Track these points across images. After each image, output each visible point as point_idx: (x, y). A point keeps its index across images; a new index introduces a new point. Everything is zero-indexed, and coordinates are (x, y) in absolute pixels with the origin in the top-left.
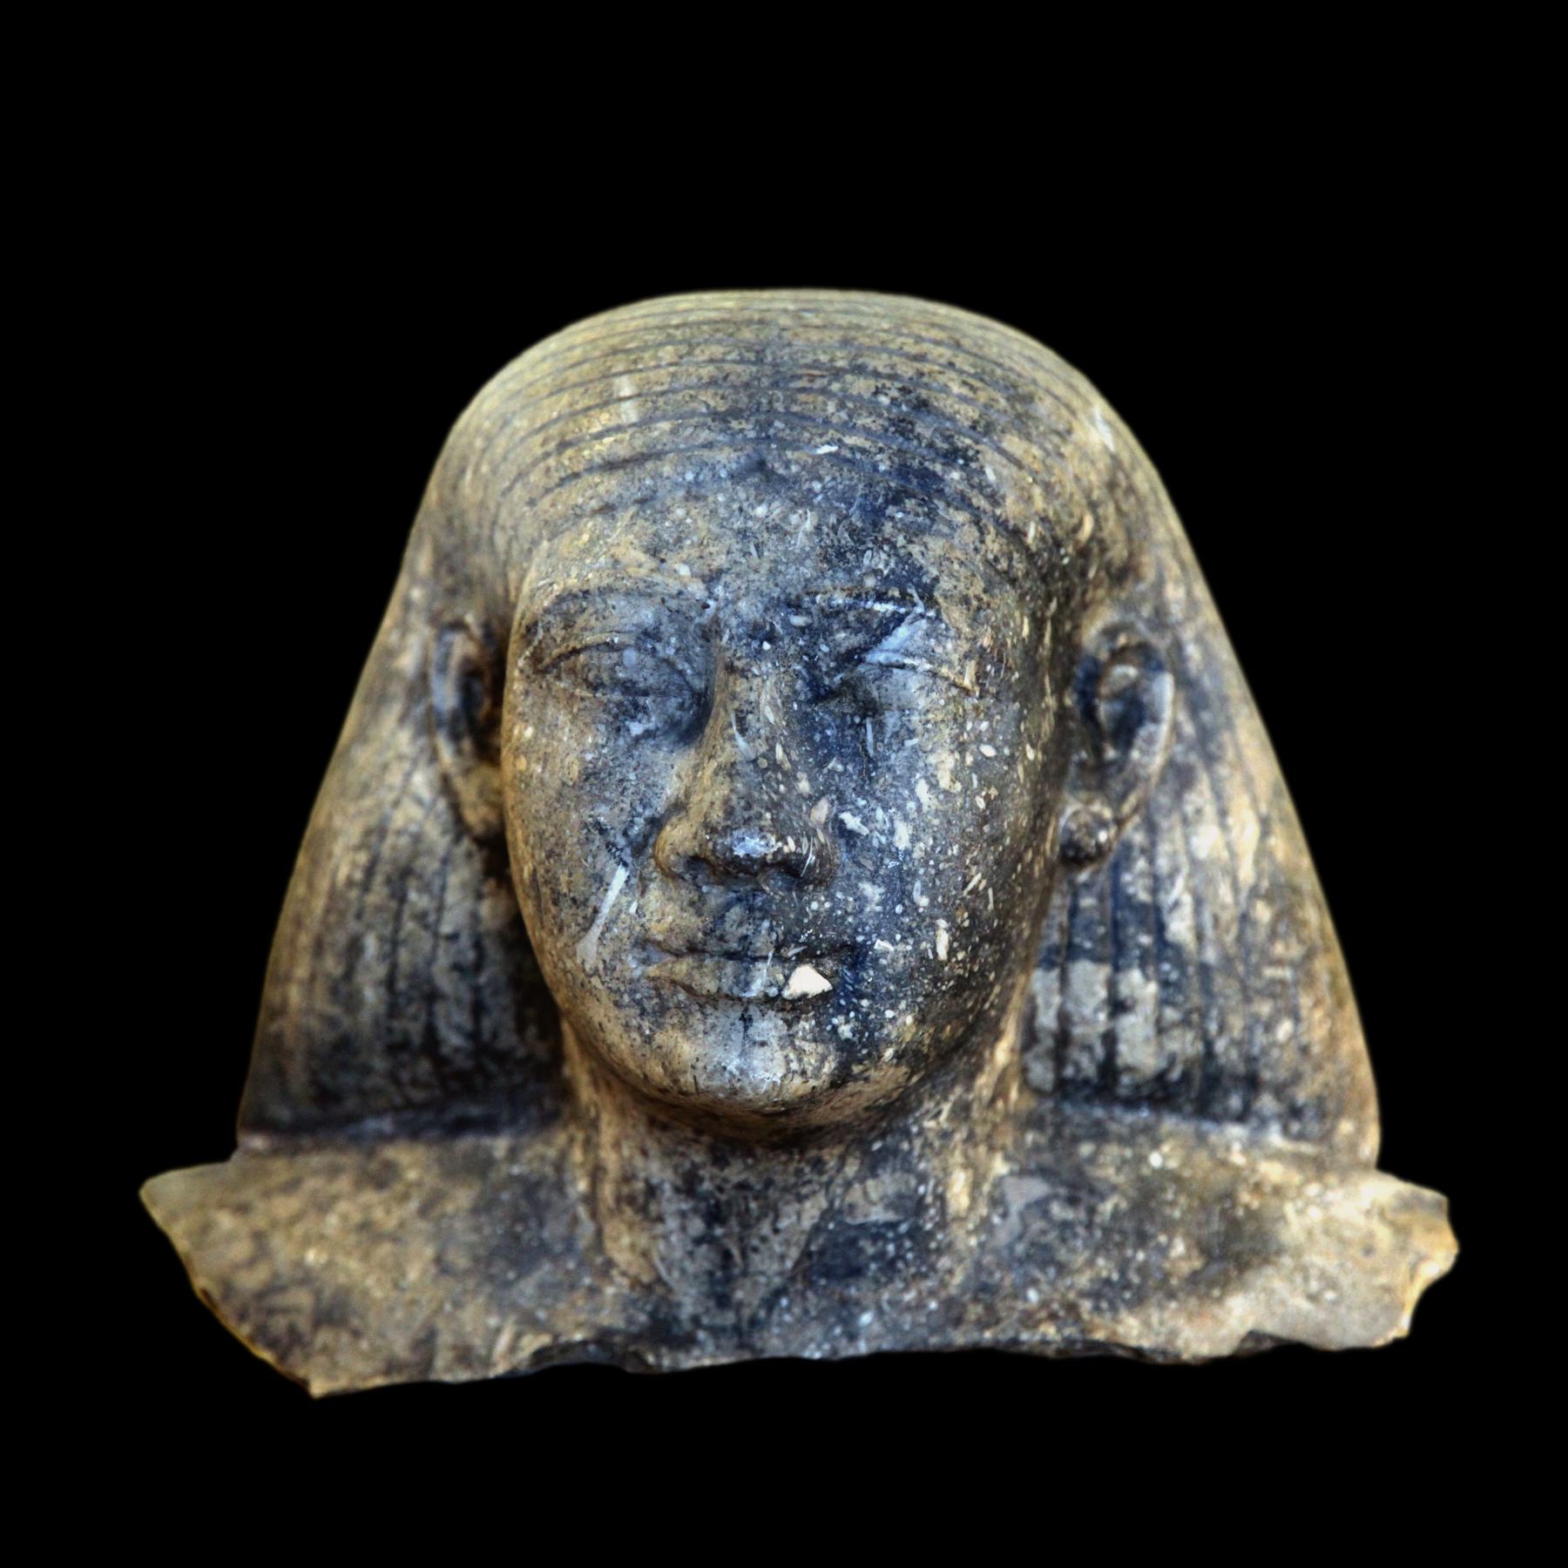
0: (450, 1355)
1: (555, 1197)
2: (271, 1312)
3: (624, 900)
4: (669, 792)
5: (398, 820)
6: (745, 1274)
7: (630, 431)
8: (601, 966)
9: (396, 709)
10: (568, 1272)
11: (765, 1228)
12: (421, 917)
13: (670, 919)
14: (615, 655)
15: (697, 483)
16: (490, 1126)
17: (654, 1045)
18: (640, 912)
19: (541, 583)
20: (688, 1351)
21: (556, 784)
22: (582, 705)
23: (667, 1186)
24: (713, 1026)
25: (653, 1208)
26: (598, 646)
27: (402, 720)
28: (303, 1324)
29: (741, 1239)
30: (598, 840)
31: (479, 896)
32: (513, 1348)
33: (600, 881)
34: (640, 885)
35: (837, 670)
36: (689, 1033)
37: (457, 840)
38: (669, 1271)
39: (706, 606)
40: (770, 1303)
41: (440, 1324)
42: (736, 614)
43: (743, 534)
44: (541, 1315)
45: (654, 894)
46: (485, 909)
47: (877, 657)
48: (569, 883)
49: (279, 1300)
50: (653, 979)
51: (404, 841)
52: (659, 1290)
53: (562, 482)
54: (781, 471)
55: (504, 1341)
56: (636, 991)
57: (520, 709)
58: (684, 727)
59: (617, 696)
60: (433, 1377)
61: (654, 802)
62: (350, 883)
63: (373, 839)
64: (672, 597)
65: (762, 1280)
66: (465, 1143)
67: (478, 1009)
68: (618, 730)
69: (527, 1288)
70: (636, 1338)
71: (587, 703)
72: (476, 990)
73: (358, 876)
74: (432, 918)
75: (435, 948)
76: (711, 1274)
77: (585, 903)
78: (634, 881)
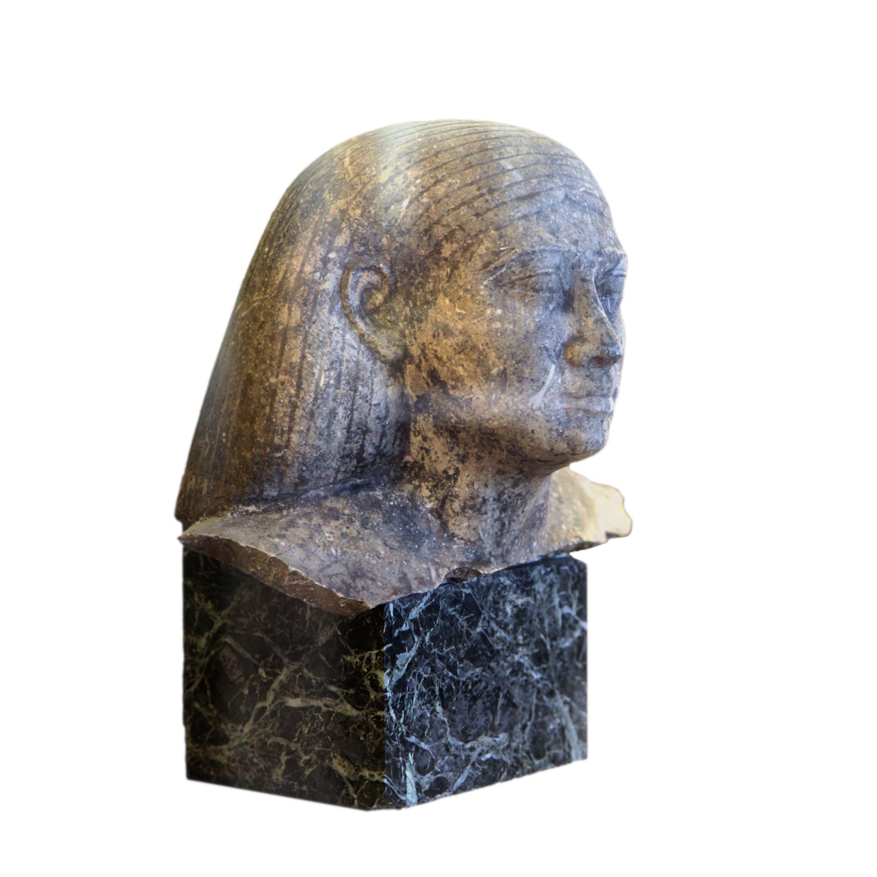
0: (416, 582)
1: (416, 513)
2: (330, 577)
3: (556, 377)
4: (568, 332)
5: (346, 355)
6: (508, 532)
7: (523, 183)
8: (543, 406)
9: (327, 307)
10: (435, 542)
11: (520, 512)
12: (364, 398)
13: (579, 383)
14: (549, 277)
15: (553, 204)
16: (368, 486)
17: (563, 436)
18: (563, 382)
19: (502, 249)
20: (490, 567)
21: (523, 332)
22: (531, 299)
23: (491, 499)
24: (593, 425)
25: (483, 509)
26: (542, 274)
27: (331, 312)
28: (350, 581)
29: (510, 517)
30: (544, 352)
31: (388, 386)
32: (438, 576)
33: (546, 371)
34: (561, 370)
35: (602, 279)
36: (583, 429)
37: (374, 363)
38: (484, 535)
39: (576, 255)
40: (513, 543)
41: (406, 571)
42: (586, 257)
43: (574, 224)
44: (437, 560)
45: (568, 373)
46: (390, 391)
47: (615, 273)
48: (530, 373)
49: (329, 571)
50: (566, 409)
51: (352, 365)
52: (479, 543)
53: (497, 206)
54: (574, 199)
55: (433, 574)
56: (558, 415)
57: (488, 302)
58: (562, 305)
59: (548, 294)
60: (414, 592)
61: (563, 337)
62: (327, 385)
63: (337, 365)
64: (566, 252)
65: (513, 533)
66: (362, 495)
67: (383, 435)
68: (546, 308)
69: (425, 550)
70: (473, 563)
71: (535, 298)
72: (384, 427)
73: (332, 382)
74: (369, 397)
75: (370, 410)
76: (497, 533)
77: (538, 380)
78: (558, 370)
